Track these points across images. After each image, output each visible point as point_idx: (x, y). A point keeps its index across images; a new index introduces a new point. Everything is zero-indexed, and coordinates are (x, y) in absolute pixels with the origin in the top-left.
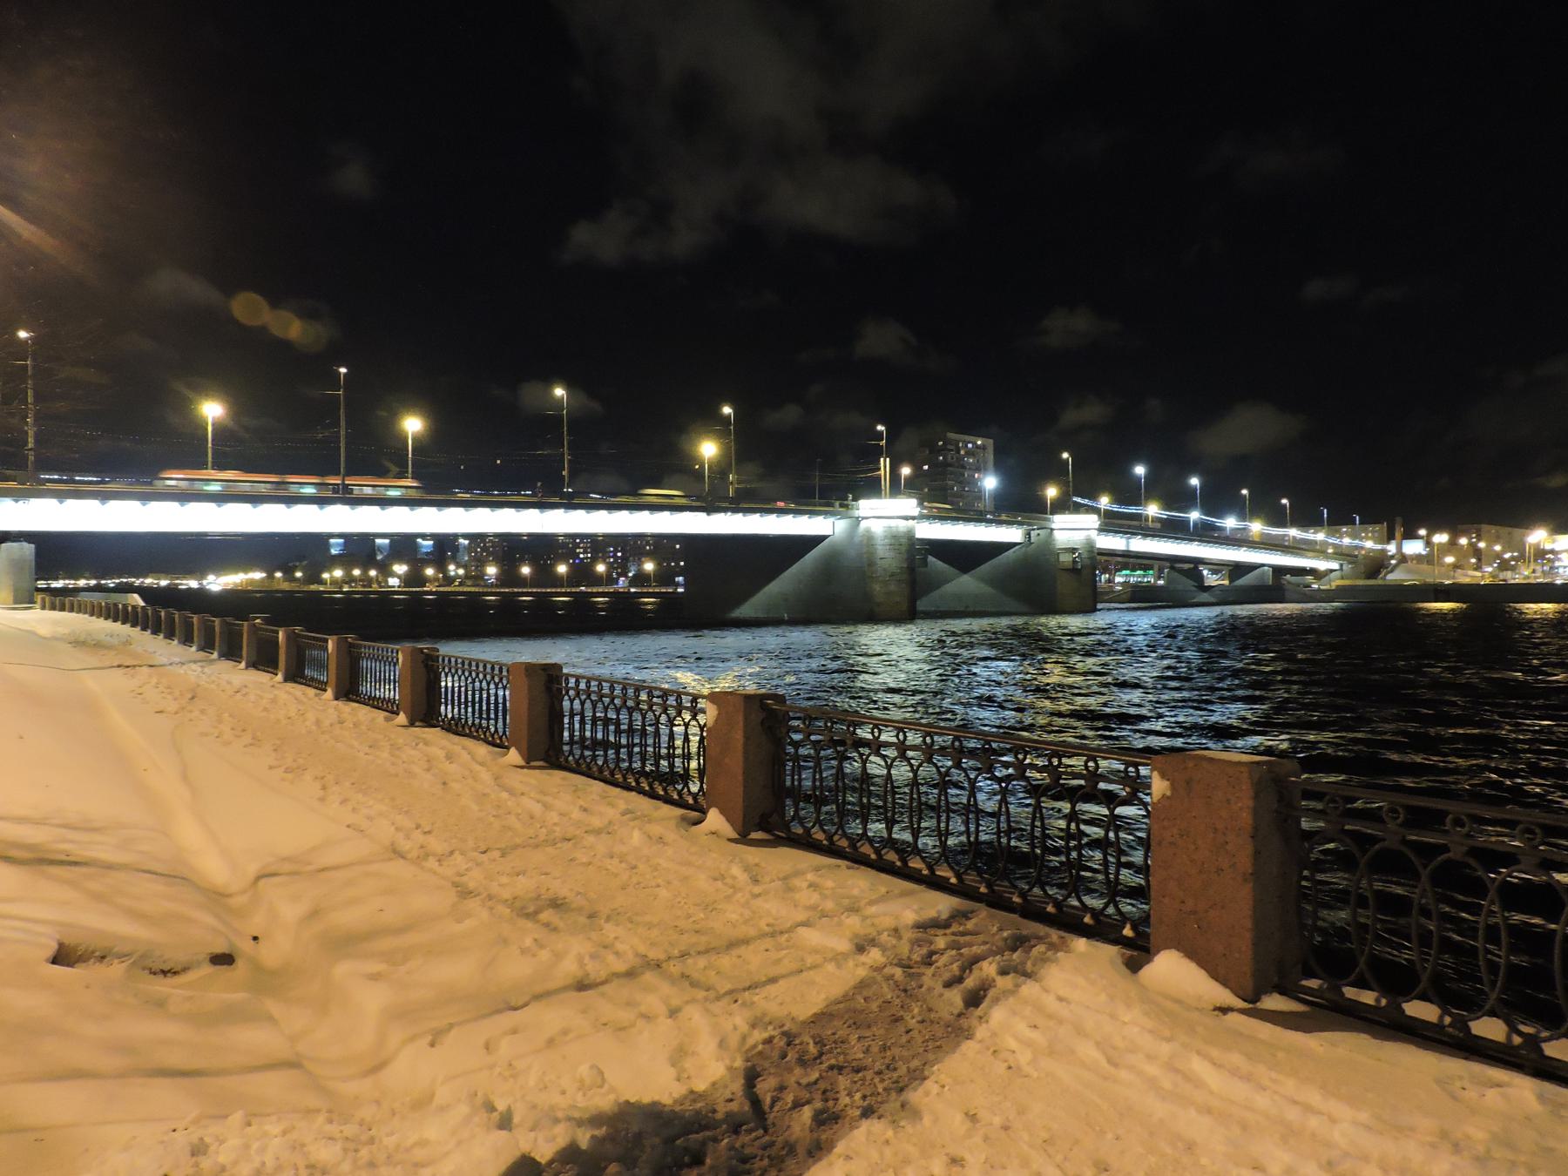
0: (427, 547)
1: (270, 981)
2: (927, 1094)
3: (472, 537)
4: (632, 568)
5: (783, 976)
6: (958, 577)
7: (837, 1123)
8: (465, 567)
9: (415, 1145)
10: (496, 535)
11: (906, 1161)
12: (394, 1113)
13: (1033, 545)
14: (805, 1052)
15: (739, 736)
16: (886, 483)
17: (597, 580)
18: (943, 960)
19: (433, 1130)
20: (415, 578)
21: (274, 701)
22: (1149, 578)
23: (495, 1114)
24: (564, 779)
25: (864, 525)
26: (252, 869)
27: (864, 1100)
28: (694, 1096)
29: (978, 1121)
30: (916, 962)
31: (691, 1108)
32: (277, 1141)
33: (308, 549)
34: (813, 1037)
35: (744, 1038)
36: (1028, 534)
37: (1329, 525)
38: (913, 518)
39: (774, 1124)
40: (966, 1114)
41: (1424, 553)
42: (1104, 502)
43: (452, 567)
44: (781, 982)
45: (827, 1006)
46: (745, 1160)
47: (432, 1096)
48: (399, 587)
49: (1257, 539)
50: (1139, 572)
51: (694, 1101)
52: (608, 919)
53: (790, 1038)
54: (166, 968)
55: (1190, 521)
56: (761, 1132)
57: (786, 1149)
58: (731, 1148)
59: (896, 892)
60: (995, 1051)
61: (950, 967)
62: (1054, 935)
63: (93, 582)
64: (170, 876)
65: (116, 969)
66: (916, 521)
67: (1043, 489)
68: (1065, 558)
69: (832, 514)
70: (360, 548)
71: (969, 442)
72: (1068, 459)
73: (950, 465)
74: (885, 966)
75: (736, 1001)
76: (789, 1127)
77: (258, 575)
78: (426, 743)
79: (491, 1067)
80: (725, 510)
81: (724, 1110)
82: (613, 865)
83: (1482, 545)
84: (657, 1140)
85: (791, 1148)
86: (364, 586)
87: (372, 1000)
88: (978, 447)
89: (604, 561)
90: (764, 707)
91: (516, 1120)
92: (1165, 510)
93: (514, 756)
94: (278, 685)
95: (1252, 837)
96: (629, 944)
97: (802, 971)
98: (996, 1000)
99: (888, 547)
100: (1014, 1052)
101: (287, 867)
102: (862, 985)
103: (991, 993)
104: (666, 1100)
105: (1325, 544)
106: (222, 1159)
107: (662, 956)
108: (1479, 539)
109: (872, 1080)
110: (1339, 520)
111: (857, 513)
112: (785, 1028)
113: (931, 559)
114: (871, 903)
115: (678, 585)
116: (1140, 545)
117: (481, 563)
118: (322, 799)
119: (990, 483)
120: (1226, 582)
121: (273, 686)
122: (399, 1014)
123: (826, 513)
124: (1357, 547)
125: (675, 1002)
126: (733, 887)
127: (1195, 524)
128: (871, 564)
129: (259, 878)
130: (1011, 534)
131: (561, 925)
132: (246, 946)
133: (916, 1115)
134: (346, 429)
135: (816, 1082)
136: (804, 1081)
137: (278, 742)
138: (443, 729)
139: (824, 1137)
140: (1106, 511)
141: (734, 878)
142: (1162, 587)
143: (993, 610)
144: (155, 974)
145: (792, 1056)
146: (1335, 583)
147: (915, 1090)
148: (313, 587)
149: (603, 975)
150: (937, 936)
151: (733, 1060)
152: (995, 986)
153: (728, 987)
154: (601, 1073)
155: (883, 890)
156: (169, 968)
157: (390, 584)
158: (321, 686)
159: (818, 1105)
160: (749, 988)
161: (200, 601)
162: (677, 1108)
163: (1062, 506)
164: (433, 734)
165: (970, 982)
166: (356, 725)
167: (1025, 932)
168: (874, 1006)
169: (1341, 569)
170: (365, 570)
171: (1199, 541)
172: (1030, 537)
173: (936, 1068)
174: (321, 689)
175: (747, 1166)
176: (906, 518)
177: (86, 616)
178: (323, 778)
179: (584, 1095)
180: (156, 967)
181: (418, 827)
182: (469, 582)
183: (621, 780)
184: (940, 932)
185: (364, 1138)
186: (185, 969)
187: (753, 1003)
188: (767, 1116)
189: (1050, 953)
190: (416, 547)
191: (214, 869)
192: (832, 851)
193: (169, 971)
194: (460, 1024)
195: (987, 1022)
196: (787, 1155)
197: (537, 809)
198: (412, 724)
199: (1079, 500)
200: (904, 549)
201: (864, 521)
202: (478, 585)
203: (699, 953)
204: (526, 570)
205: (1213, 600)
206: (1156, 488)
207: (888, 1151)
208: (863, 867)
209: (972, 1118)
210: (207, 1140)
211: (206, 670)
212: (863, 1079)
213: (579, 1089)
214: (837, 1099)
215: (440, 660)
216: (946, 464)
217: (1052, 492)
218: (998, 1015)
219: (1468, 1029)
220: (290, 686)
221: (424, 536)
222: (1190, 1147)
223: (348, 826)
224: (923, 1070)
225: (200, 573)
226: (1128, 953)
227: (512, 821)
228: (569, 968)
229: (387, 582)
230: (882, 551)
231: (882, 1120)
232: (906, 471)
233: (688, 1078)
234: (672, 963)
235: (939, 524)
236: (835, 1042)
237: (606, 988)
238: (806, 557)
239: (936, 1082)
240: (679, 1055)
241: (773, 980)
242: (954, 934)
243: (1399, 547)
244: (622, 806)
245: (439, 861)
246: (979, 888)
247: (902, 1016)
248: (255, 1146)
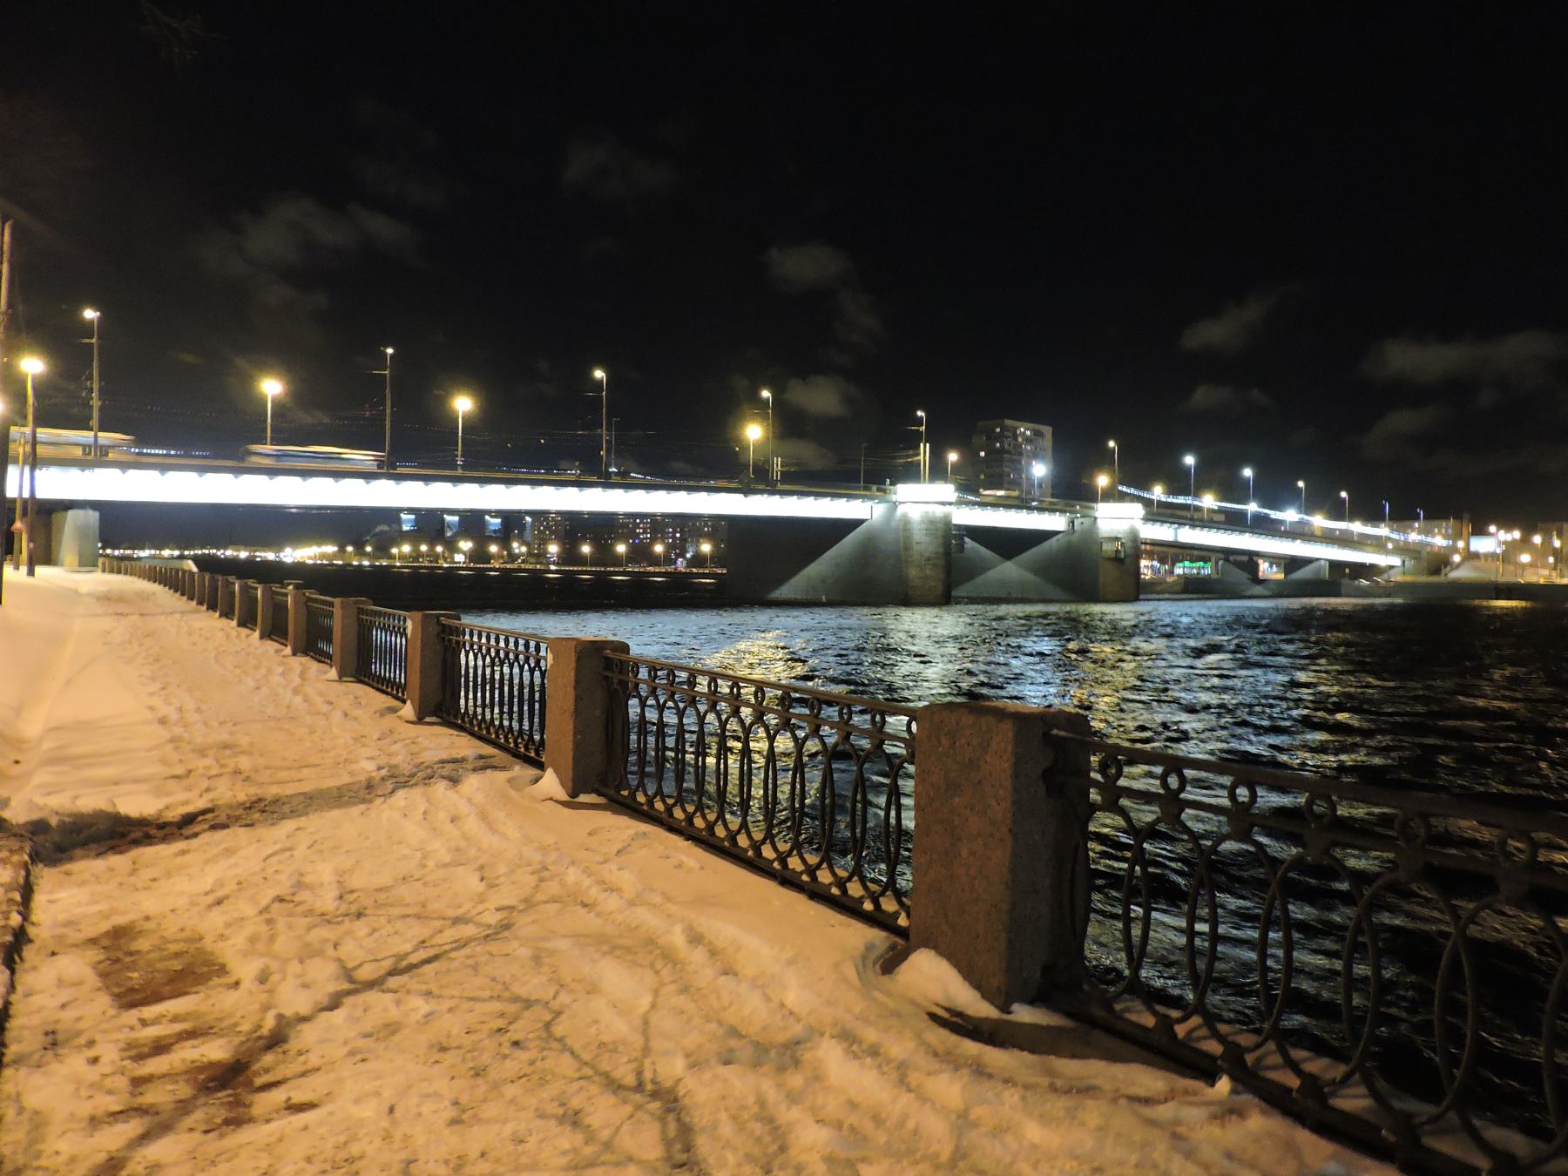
0: (495, 524)
3: (536, 514)
4: (690, 549)
8: (527, 544)
10: (558, 513)
17: (655, 560)
20: (479, 555)
22: (1207, 570)
25: (901, 510)
37: (1390, 519)
38: (950, 504)
41: (1499, 551)
42: (1158, 492)
43: (515, 545)
48: (464, 563)
49: (1318, 533)
67: (1092, 477)
68: (1108, 548)
69: (871, 498)
70: (430, 524)
77: (330, 549)
80: (761, 492)
86: (431, 562)
89: (663, 541)
92: (1221, 501)
105: (1389, 539)
110: (1402, 516)
111: (894, 498)
117: (544, 542)
120: (1281, 576)
128: (907, 548)
130: (1055, 522)
146: (1397, 577)
163: (1111, 495)
170: (432, 545)
176: (943, 504)
182: (533, 560)
190: (483, 524)
199: (1124, 489)
200: (940, 533)
202: (541, 563)
204: (586, 549)
205: (1266, 593)
216: (1002, 451)
217: (1103, 481)
221: (489, 512)
225: (277, 544)
229: (453, 558)
230: (920, 538)
243: (1468, 545)
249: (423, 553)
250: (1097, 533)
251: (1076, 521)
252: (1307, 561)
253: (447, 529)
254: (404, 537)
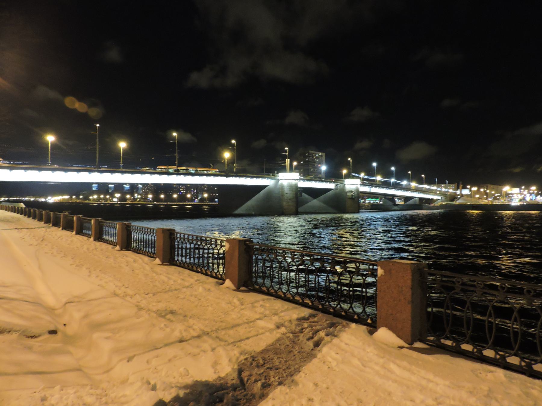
0: (127, 188)
1: (70, 340)
2: (301, 377)
3: (145, 185)
5: (251, 337)
6: (312, 200)
7: (269, 387)
8: (140, 195)
9: (122, 396)
10: (152, 184)
11: (293, 400)
12: (114, 386)
13: (338, 190)
14: (259, 363)
15: (236, 254)
16: (288, 167)
18: (306, 331)
19: (128, 391)
20: (122, 199)
21: (72, 241)
23: (150, 385)
24: (175, 269)
25: (280, 182)
26: (64, 300)
27: (279, 379)
28: (220, 378)
29: (318, 386)
30: (297, 332)
31: (219, 382)
32: (72, 396)
33: (86, 187)
34: (262, 358)
35: (238, 358)
36: (337, 186)
38: (297, 180)
39: (248, 388)
40: (314, 384)
42: (362, 175)
43: (136, 195)
44: (251, 339)
45: (267, 347)
46: (238, 400)
47: (128, 379)
48: (117, 201)
50: (374, 199)
51: (220, 380)
52: (191, 317)
53: (254, 358)
54: (32, 335)
55: (391, 182)
56: (243, 390)
57: (252, 396)
58: (233, 396)
59: (291, 308)
60: (324, 362)
61: (309, 333)
62: (344, 322)
63: (6, 199)
64: (35, 303)
65: (14, 336)
66: (298, 181)
67: (342, 170)
68: (349, 194)
69: (270, 178)
70: (103, 188)
71: (317, 154)
72: (350, 160)
73: (310, 162)
74: (286, 333)
75: (235, 346)
76: (253, 388)
78: (127, 257)
79: (149, 369)
80: (232, 176)
81: (231, 383)
82: (192, 299)
83: (488, 191)
84: (207, 394)
85: (253, 396)
87: (107, 346)
88: (320, 156)
90: (245, 244)
91: (158, 387)
93: (158, 261)
94: (73, 236)
95: (411, 289)
96: (198, 326)
97: (258, 335)
98: (325, 345)
99: (289, 190)
100: (330, 362)
101: (76, 300)
102: (279, 340)
103: (323, 342)
104: (210, 380)
105: (436, 190)
106: (53, 402)
107: (209, 331)
108: (487, 189)
109: (282, 372)
110: (441, 182)
112: (252, 355)
113: (303, 194)
114: (282, 312)
115: (215, 202)
116: (374, 190)
117: (147, 194)
118: (89, 276)
119: (324, 168)
121: (72, 236)
122: (116, 351)
123: (267, 178)
124: (447, 192)
125: (214, 346)
126: (234, 306)
127: (393, 183)
128: (283, 195)
129: (66, 303)
131: (174, 319)
132: (61, 327)
133: (296, 384)
134: (99, 146)
135: (262, 373)
136: (258, 373)
137: (74, 256)
138: (133, 251)
139: (265, 392)
140: (363, 178)
141: (235, 303)
142: (381, 204)
143: (324, 211)
144: (28, 337)
145: (254, 364)
147: (296, 375)
148: (86, 201)
149: (189, 337)
150: (304, 323)
151: (234, 366)
152: (324, 340)
153: (232, 341)
154: (188, 371)
155: (286, 307)
156: (34, 335)
157: (114, 201)
158: (89, 236)
159: (263, 381)
160: (240, 341)
161: (45, 206)
162: (214, 383)
163: (348, 176)
164: (130, 254)
165: (316, 338)
166: (102, 250)
167: (334, 321)
168: (283, 347)
169: (441, 199)
170: (105, 195)
171: (394, 189)
173: (304, 368)
174: (89, 237)
175: (238, 402)
177: (4, 211)
178: (89, 268)
179: (182, 378)
180: (29, 335)
181: (123, 286)
182: (142, 200)
183: (195, 269)
184: (306, 321)
185: (104, 394)
186: (39, 336)
187: (241, 346)
188: (245, 385)
189: (343, 328)
190: (123, 188)
191: (50, 300)
192: (268, 294)
193: (33, 336)
194: (139, 354)
195: (321, 352)
196: (252, 398)
197: (166, 279)
198: (121, 250)
199: (354, 174)
200: (294, 190)
201: (281, 180)
203: (222, 329)
206: (380, 170)
207: (287, 397)
208: (279, 299)
209: (316, 385)
210: (47, 396)
211: (47, 230)
212: (279, 372)
213: (180, 376)
214: (270, 379)
215: (132, 228)
217: (345, 172)
218: (324, 350)
219: (482, 353)
220: (78, 236)
221: (126, 184)
222: (390, 394)
223: (99, 285)
224: (299, 369)
226: (369, 328)
227: (157, 283)
228: (177, 334)
229: (113, 200)
230: (287, 191)
231: (285, 386)
232: (295, 163)
233: (218, 372)
234: (213, 333)
235: (306, 182)
236: (269, 359)
237: (190, 341)
238: (260, 193)
239: (304, 373)
240: (215, 364)
241: (248, 338)
242: (310, 322)
243: (461, 192)
244: (196, 278)
245: (131, 297)
246: (319, 306)
247: (292, 350)
248: (65, 397)
249: (102, 198)
252: (412, 198)
253: (110, 190)
254: (94, 192)
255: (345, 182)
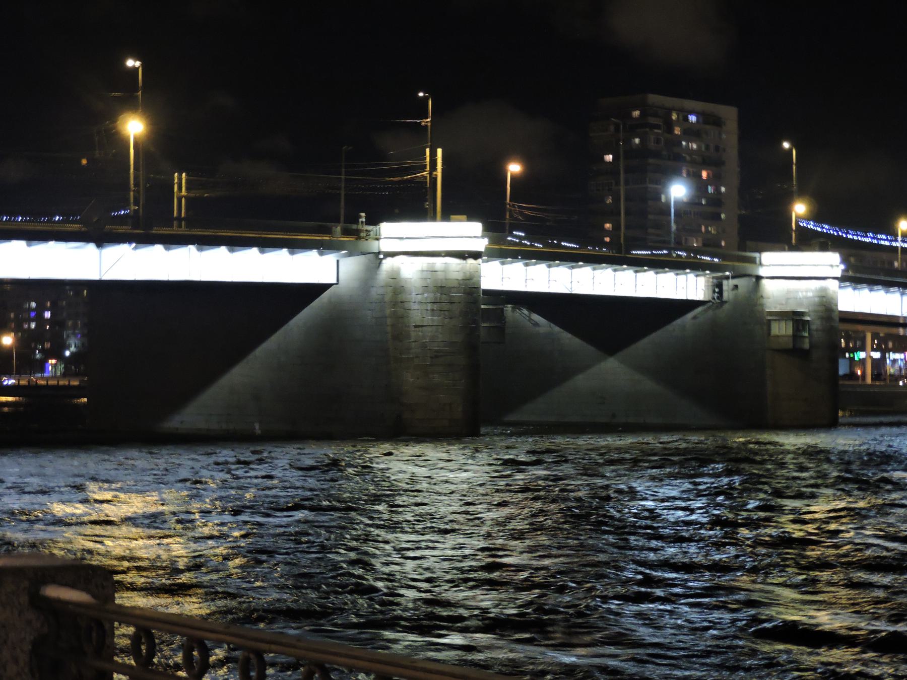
13: (726, 306)
25: (388, 264)
36: (718, 286)
38: (476, 255)
111: (374, 246)
172: (721, 293)
201: (389, 259)
250: (762, 305)
251: (725, 282)
255: (761, 264)
